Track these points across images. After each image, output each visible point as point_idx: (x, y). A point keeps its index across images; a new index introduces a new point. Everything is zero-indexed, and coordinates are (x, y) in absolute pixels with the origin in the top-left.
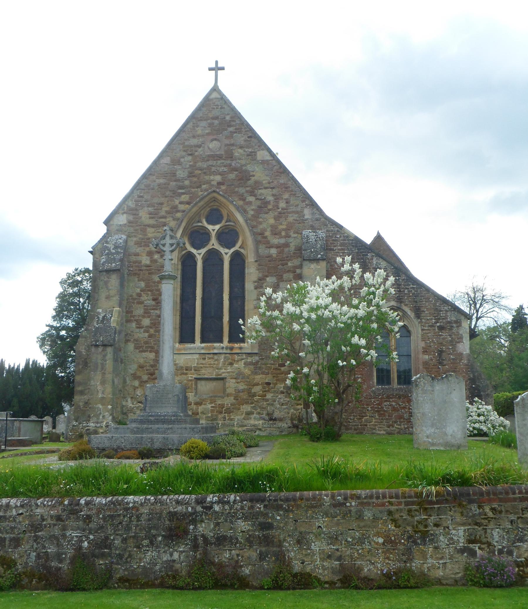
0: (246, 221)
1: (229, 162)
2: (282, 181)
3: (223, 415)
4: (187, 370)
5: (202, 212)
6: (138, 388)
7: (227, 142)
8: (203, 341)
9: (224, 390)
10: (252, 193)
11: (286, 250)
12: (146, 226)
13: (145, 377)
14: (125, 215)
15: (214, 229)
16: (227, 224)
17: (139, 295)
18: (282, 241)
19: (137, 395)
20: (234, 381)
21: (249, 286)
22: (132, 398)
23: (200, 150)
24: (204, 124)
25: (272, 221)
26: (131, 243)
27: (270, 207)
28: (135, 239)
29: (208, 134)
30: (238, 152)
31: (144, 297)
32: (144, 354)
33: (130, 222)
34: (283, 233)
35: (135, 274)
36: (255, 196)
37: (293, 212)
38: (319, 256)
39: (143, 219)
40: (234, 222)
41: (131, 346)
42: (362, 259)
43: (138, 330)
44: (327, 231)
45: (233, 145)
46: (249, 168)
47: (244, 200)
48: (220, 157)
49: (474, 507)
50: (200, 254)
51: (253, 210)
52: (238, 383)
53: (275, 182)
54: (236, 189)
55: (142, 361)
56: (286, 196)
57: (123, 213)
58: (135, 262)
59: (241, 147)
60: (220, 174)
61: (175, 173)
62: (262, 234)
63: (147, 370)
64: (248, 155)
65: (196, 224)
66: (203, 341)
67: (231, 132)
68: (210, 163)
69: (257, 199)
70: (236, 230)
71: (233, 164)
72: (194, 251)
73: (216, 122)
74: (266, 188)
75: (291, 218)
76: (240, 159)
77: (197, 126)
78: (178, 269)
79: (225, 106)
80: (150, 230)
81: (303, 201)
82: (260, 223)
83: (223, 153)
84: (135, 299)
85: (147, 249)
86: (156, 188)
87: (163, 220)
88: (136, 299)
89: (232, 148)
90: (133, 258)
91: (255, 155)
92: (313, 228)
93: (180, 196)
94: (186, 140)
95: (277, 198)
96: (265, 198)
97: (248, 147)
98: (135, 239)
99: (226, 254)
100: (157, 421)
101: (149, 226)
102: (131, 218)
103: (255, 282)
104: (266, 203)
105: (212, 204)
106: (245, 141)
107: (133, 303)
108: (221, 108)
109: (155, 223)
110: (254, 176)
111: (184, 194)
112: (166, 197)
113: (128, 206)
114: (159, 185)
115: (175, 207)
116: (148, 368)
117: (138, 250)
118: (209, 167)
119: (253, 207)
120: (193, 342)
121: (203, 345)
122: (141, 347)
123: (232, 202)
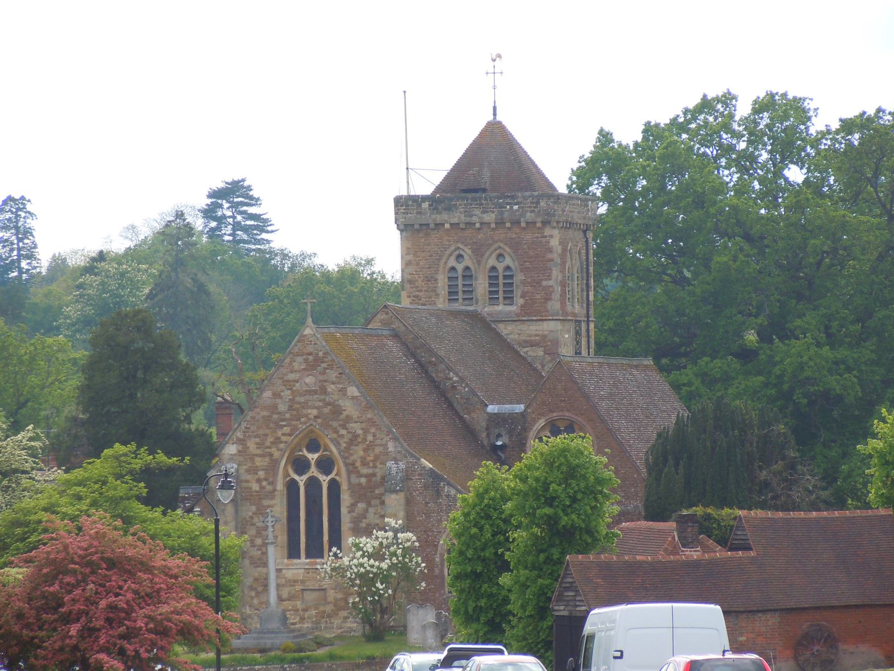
0: (340, 453)
1: (323, 397)
2: (369, 416)
3: (325, 619)
4: (294, 582)
5: (302, 442)
6: (254, 597)
7: (321, 378)
8: (307, 557)
9: (325, 599)
10: (344, 427)
11: (374, 479)
12: (253, 455)
13: (260, 589)
14: (235, 445)
15: (313, 457)
16: (324, 453)
17: (252, 518)
18: (370, 471)
20: (333, 591)
21: (344, 510)
22: (250, 606)
23: (298, 384)
24: (299, 359)
25: (361, 453)
26: (242, 471)
27: (360, 440)
28: (245, 467)
29: (304, 369)
30: (331, 388)
31: (256, 520)
32: (259, 569)
33: (239, 451)
34: (371, 464)
35: (247, 499)
36: (346, 429)
37: (379, 445)
38: (398, 488)
39: (251, 449)
40: (330, 452)
41: (247, 562)
42: (436, 487)
44: (407, 462)
45: (326, 381)
46: (341, 403)
47: (337, 432)
48: (315, 392)
49: (374, 667)
50: (302, 481)
51: (345, 442)
52: (336, 593)
53: (364, 417)
54: (331, 423)
55: (256, 575)
56: (373, 430)
57: (233, 444)
58: (246, 488)
59: (333, 383)
60: (316, 408)
61: (277, 407)
62: (353, 464)
64: (339, 391)
65: (298, 453)
66: (307, 557)
67: (324, 368)
68: (307, 397)
69: (348, 432)
70: (332, 459)
71: (327, 400)
72: (296, 477)
73: (311, 358)
74: (356, 422)
75: (378, 450)
76: (333, 394)
77: (294, 361)
78: (283, 494)
79: (318, 343)
80: (257, 459)
81: (388, 435)
82: (352, 455)
83: (318, 389)
84: (247, 521)
85: (256, 477)
86: (261, 420)
87: (268, 450)
89: (325, 384)
90: (245, 485)
91: (346, 391)
92: (396, 460)
93: (282, 428)
94: (285, 375)
95: (366, 431)
96: (355, 432)
97: (339, 383)
98: (245, 467)
99: (324, 481)
100: (268, 632)
101: (257, 455)
102: (240, 448)
103: (348, 507)
104: (356, 436)
105: (310, 435)
106: (336, 377)
107: (247, 525)
108: (314, 344)
109: (261, 453)
110: (345, 410)
111: (284, 426)
112: (270, 428)
113: (237, 437)
114: (263, 417)
115: (278, 438)
117: (249, 477)
118: (306, 402)
119: (346, 440)
120: (299, 557)
121: (308, 561)
122: (255, 563)
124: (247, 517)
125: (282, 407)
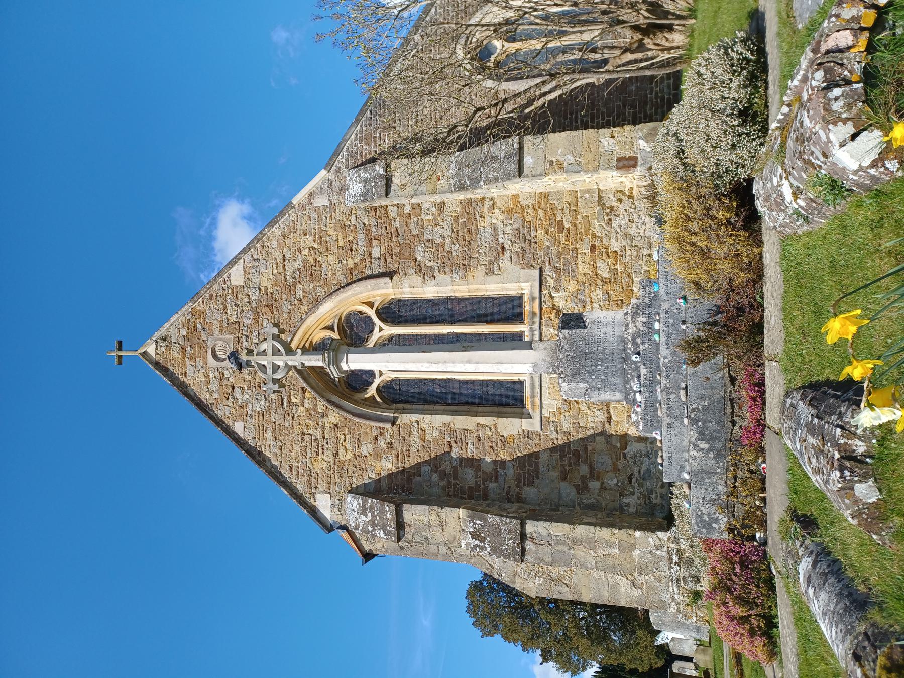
6: (602, 483)
7: (216, 332)
14: (318, 496)
18: (362, 237)
19: (617, 484)
21: (431, 291)
43: (501, 479)
55: (555, 474)
63: (570, 464)
84: (449, 483)
88: (448, 480)
99: (381, 330)
116: (566, 462)
123: (302, 321)
124: (442, 483)
125: (261, 405)
